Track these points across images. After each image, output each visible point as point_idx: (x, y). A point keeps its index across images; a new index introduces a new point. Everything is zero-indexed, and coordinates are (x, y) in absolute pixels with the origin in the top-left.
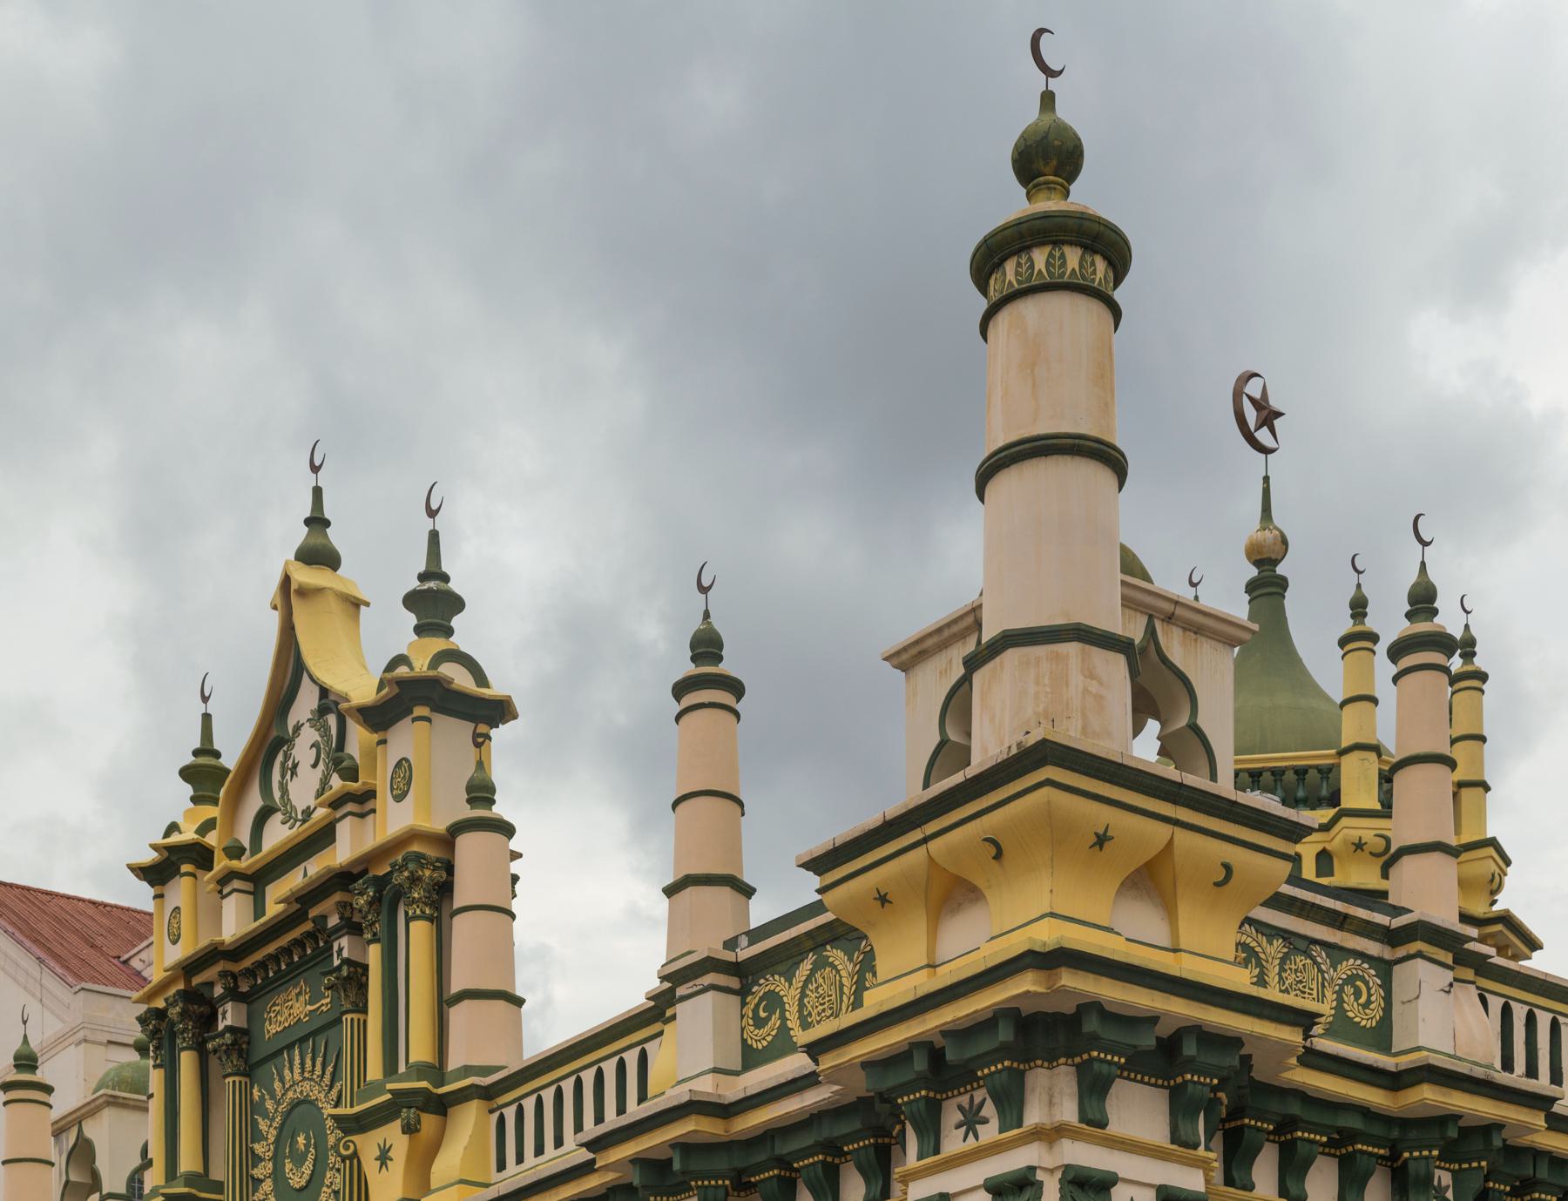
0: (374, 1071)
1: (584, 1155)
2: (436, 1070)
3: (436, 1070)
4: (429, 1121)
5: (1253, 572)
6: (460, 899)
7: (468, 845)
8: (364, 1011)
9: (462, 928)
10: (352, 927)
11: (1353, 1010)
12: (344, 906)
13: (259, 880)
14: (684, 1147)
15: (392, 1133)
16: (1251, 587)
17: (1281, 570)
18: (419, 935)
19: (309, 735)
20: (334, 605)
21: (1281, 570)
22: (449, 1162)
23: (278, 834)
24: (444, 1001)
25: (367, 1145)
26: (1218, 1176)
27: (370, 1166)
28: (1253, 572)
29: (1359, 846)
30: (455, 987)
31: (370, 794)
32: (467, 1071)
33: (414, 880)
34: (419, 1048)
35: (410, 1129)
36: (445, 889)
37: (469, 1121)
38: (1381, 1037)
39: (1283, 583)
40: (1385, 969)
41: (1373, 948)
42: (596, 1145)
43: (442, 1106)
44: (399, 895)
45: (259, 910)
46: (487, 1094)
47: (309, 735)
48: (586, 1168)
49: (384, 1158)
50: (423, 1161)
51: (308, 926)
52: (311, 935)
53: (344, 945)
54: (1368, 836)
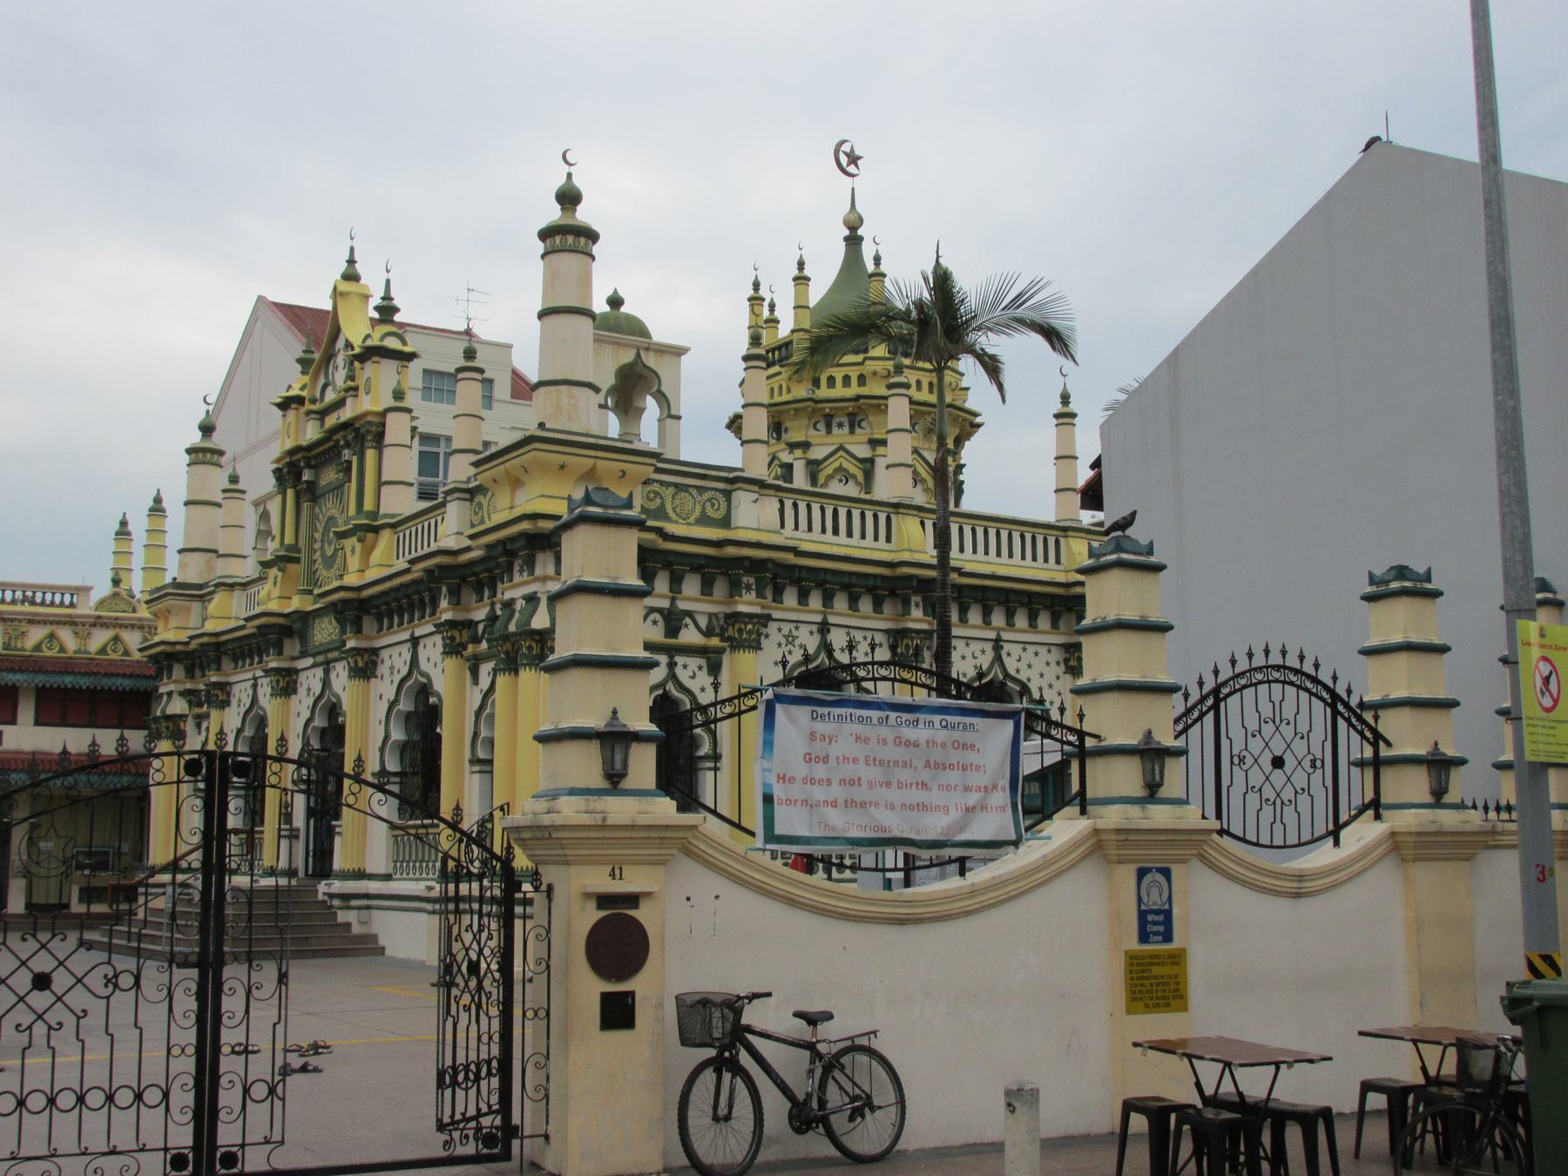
1: (407, 565)
2: (375, 514)
3: (375, 514)
4: (370, 536)
5: (847, 232)
6: (388, 440)
7: (391, 417)
9: (387, 452)
12: (345, 437)
14: (440, 567)
15: (353, 541)
16: (846, 239)
17: (860, 232)
18: (370, 454)
21: (860, 232)
22: (377, 556)
27: (349, 554)
28: (847, 232)
29: (875, 373)
30: (384, 479)
32: (386, 516)
33: (369, 432)
34: (368, 505)
35: (360, 540)
36: (381, 435)
37: (386, 537)
39: (861, 239)
42: (411, 562)
43: (376, 530)
46: (393, 526)
48: (407, 571)
49: (353, 551)
51: (331, 444)
52: (331, 448)
54: (878, 369)
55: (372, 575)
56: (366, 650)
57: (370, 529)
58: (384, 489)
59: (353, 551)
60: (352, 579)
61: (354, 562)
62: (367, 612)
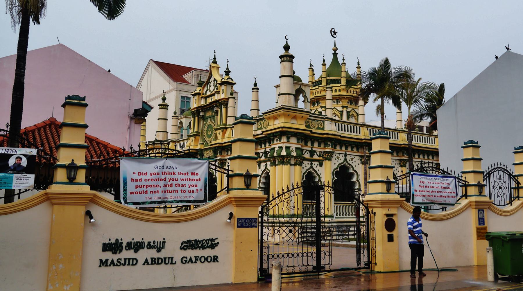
0: (219, 124)
2: (226, 124)
3: (226, 124)
4: (225, 130)
8: (218, 115)
10: (217, 106)
11: (320, 126)
13: (206, 98)
15: (220, 131)
18: (224, 109)
19: (212, 83)
20: (215, 68)
22: (227, 135)
23: (208, 93)
24: (227, 117)
25: (218, 132)
26: (303, 144)
27: (218, 134)
31: (219, 92)
32: (229, 125)
38: (323, 129)
40: (323, 122)
41: (322, 120)
43: (226, 128)
44: (222, 104)
45: (206, 103)
47: (212, 83)
49: (219, 134)
50: (224, 134)
53: (216, 109)
55: (225, 140)
56: (223, 159)
57: (224, 128)
58: (228, 118)
59: (219, 134)
60: (219, 141)
61: (220, 137)
62: (224, 150)
